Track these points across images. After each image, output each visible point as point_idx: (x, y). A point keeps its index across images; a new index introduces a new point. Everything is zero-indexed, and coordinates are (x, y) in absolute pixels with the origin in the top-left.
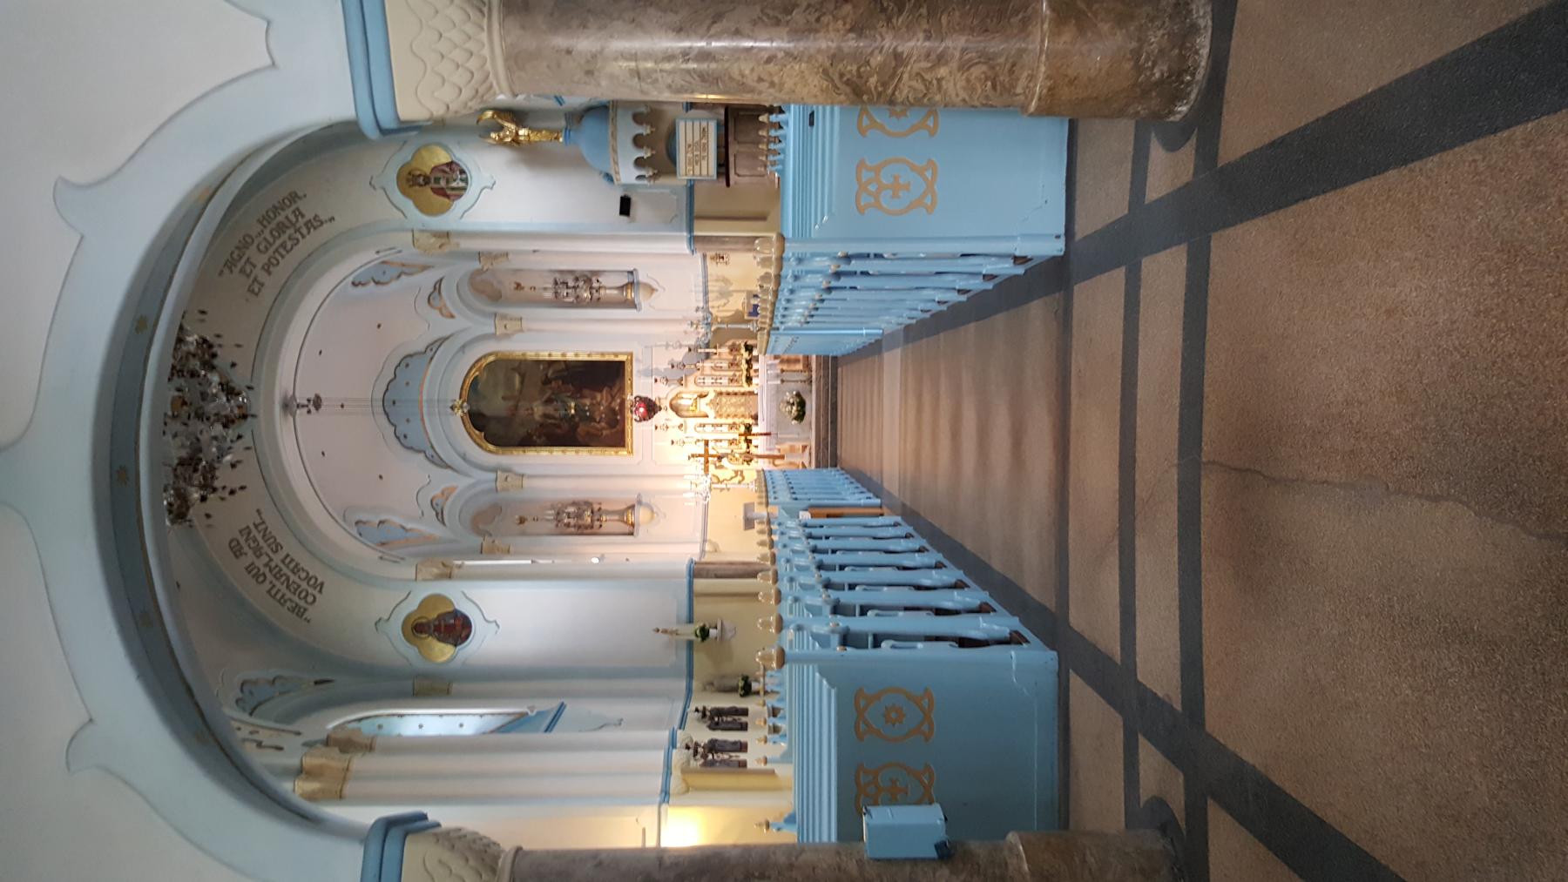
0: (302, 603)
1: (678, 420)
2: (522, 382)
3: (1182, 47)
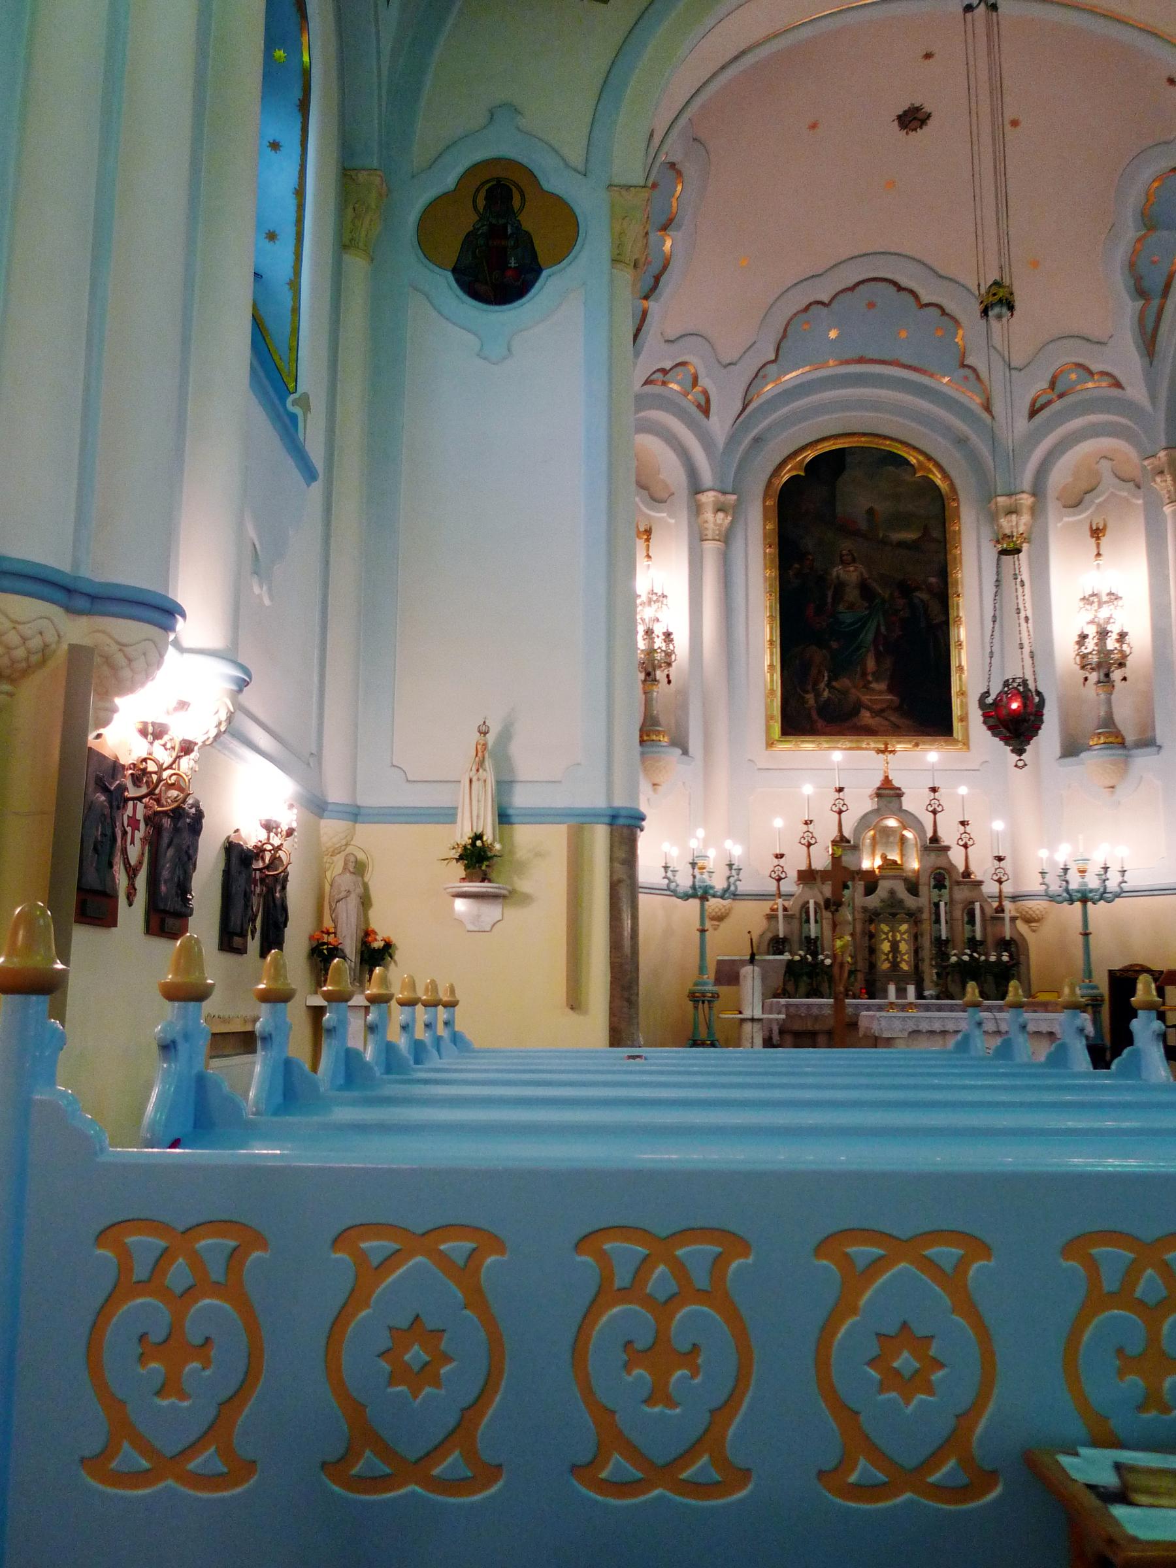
2: (901, 544)
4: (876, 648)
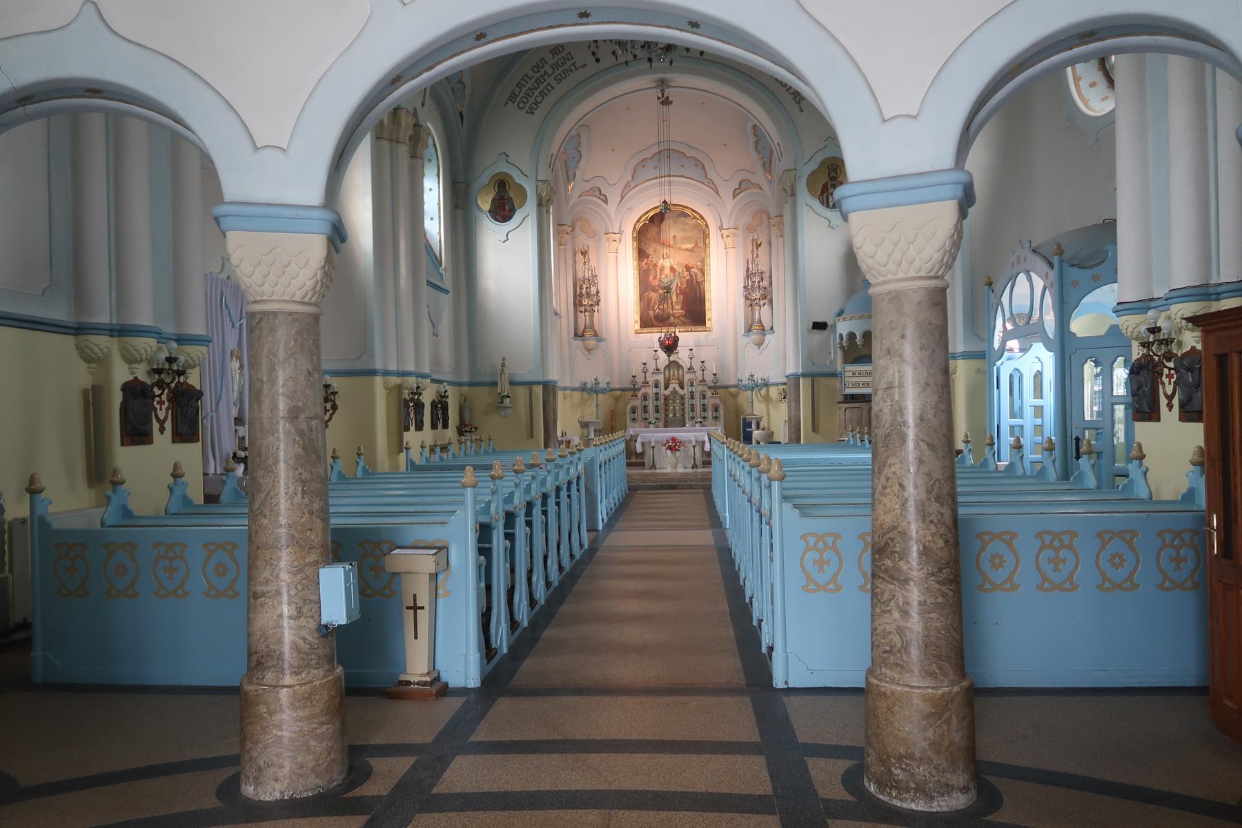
0: (518, 99)
1: (662, 366)
2: (686, 250)
3: (916, 790)
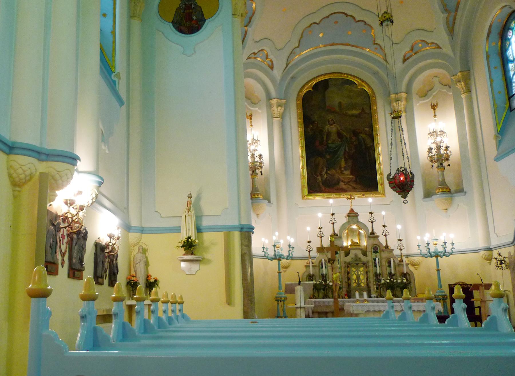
2: (353, 116)
4: (345, 157)
